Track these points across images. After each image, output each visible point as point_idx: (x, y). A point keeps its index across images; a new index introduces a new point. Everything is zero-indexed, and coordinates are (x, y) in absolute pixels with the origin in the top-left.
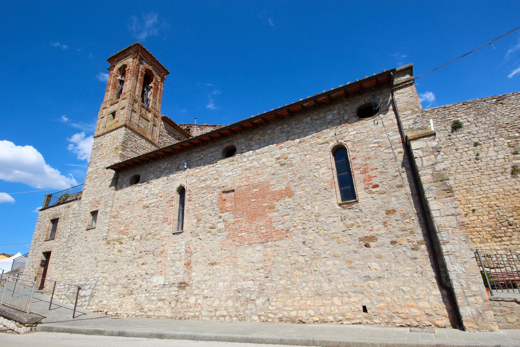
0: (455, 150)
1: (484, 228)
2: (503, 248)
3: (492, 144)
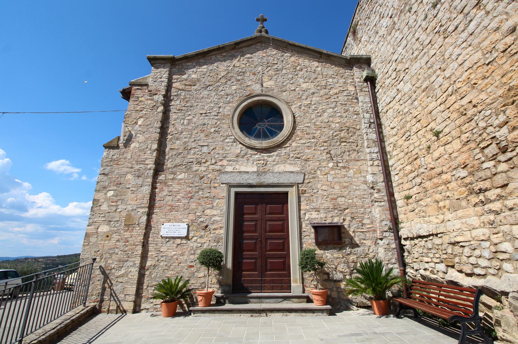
0: (408, 13)
1: (454, 172)
2: (485, 221)
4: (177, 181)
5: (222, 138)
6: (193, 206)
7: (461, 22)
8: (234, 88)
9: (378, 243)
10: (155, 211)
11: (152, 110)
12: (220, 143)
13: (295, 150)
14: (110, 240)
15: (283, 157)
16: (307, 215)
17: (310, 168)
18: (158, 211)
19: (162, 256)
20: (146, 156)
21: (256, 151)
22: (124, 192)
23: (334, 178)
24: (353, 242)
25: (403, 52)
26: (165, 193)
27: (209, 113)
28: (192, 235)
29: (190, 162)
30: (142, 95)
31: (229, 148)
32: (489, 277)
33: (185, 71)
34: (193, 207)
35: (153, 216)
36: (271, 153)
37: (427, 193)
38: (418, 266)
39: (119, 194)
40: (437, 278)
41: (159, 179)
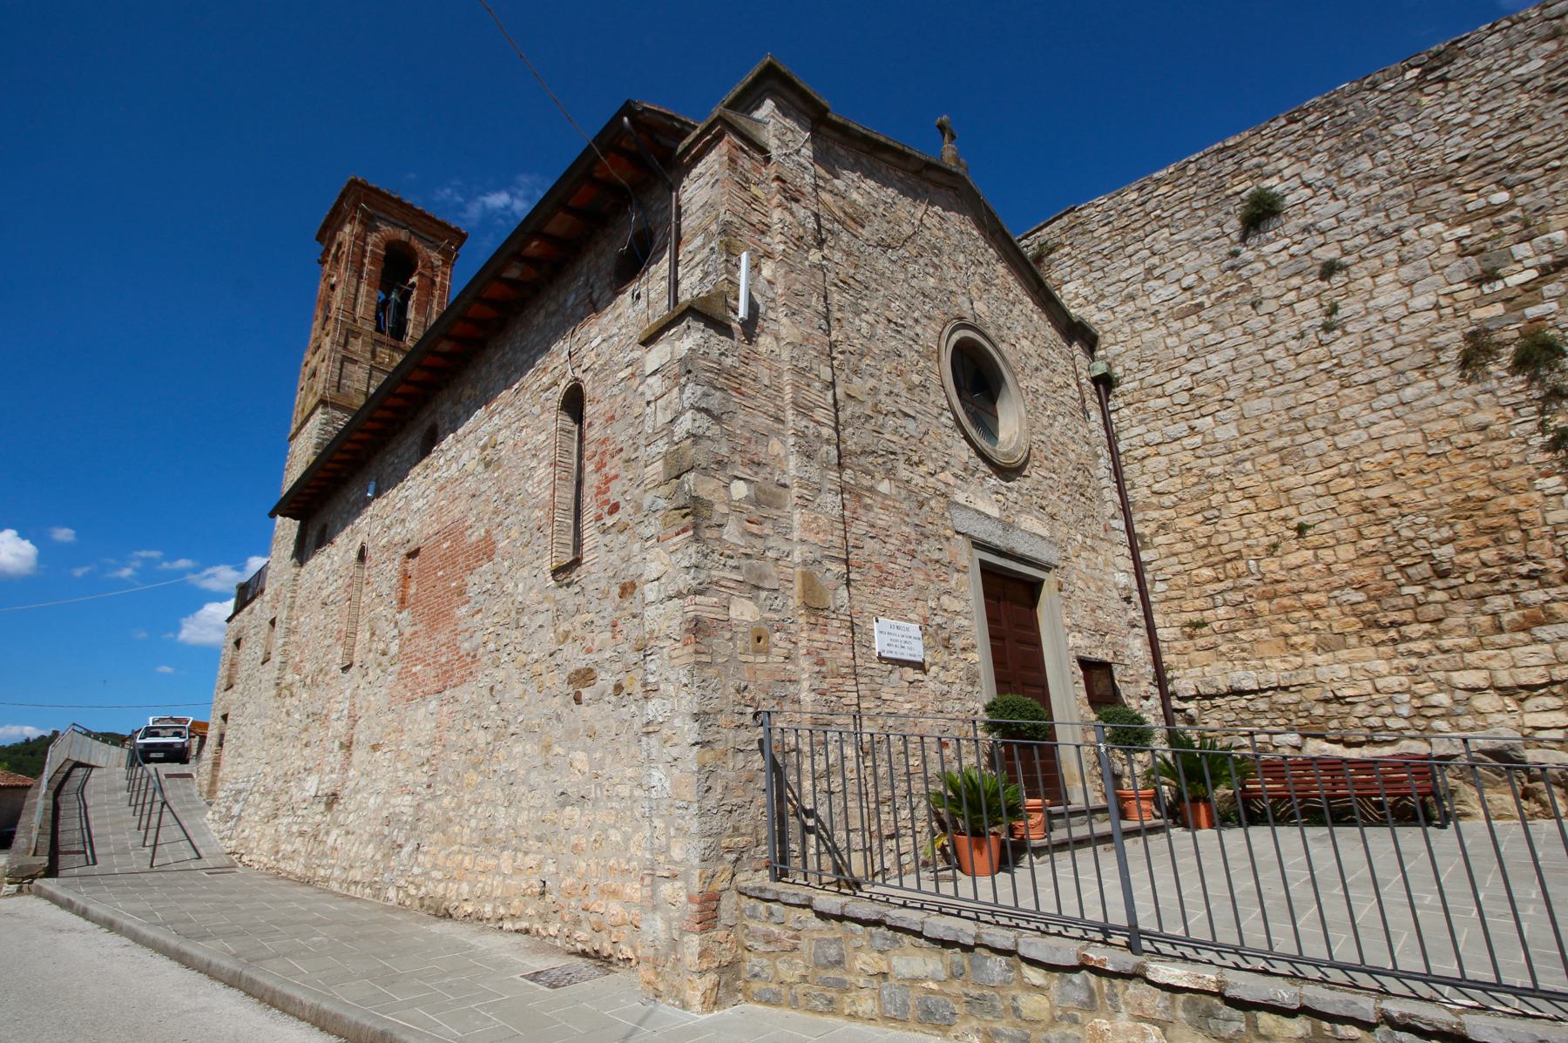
0: (1249, 307)
1: (1336, 593)
2: (1401, 666)
3: (1392, 257)
25: (1225, 367)
37: (1259, 619)
39: (763, 497)
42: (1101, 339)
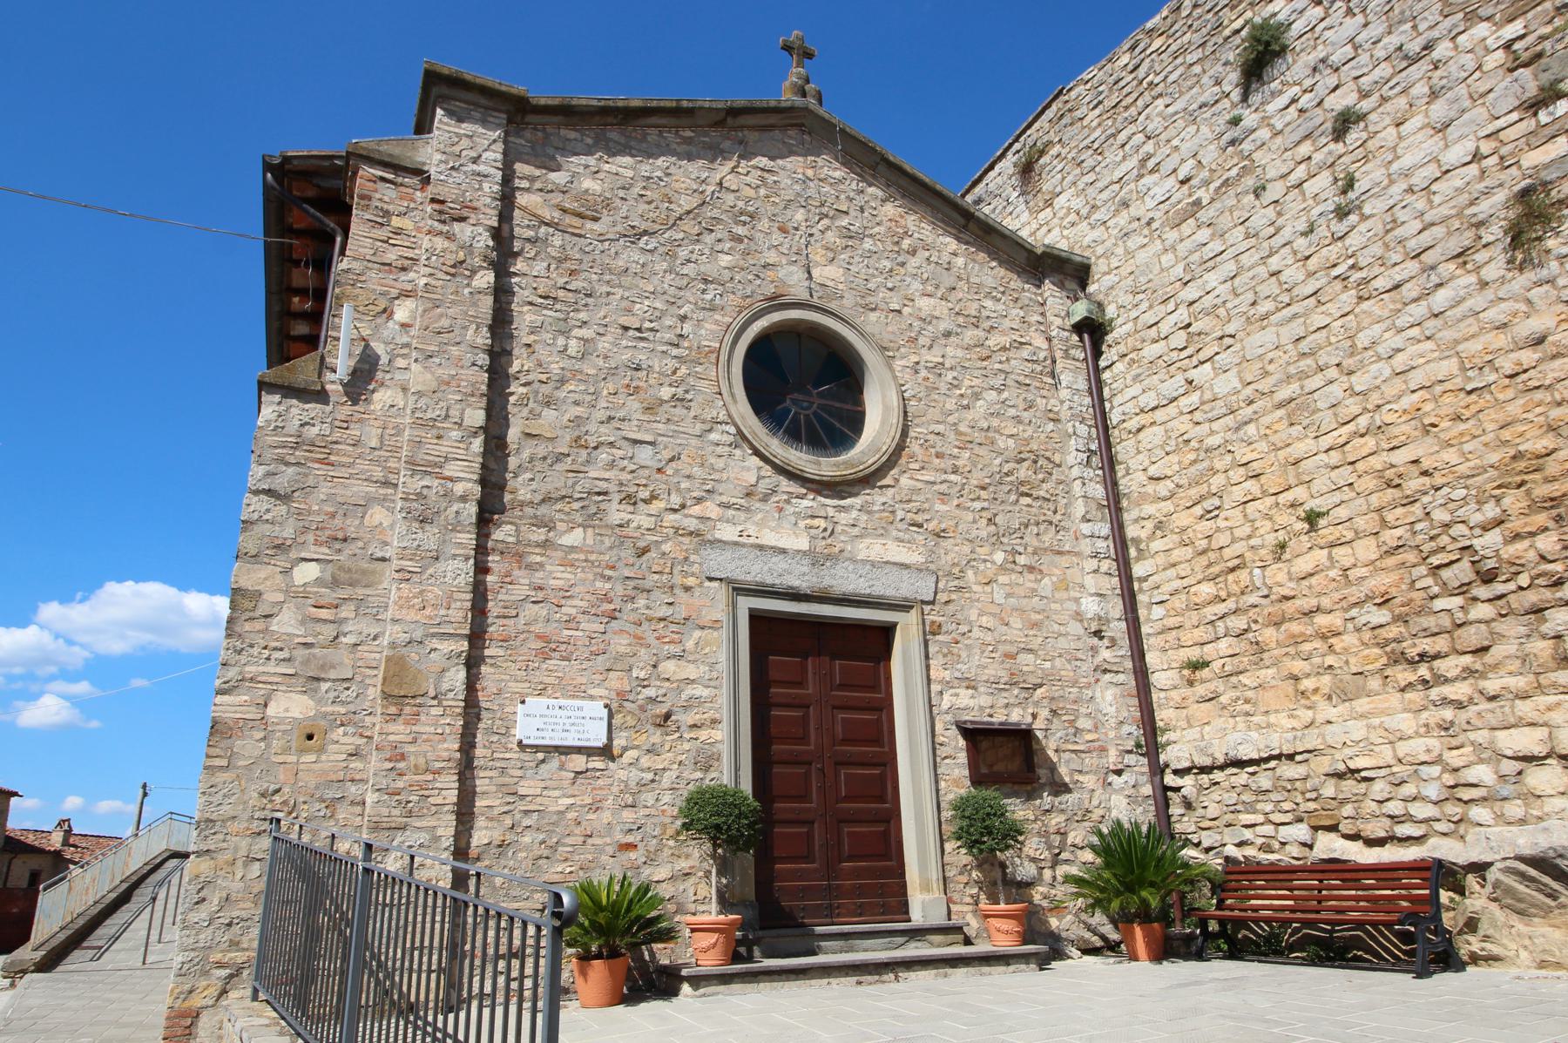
0: (1252, 197)
1: (1354, 612)
2: (1432, 722)
3: (1421, 89)
4: (559, 554)
5: (699, 427)
6: (621, 644)
7: (1412, 278)
8: (725, 260)
9: (1110, 784)
10: (487, 652)
11: (453, 275)
12: (694, 442)
13: (910, 501)
14: (321, 750)
15: (877, 515)
16: (946, 697)
17: (949, 558)
18: (501, 652)
19: (526, 812)
20: (444, 448)
21: (802, 486)
22: (364, 572)
23: (1008, 596)
24: (1057, 780)
25: (1223, 289)
26: (520, 591)
27: (652, 330)
28: (623, 743)
29: (599, 494)
30: (403, 209)
31: (720, 464)
32: (1432, 841)
33: (559, 158)
34: (622, 649)
35: (483, 668)
36: (844, 498)
37: (1265, 655)
38: (1218, 837)
39: (343, 576)
40: (1279, 860)
41: (494, 537)
42: (1094, 268)
